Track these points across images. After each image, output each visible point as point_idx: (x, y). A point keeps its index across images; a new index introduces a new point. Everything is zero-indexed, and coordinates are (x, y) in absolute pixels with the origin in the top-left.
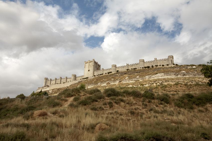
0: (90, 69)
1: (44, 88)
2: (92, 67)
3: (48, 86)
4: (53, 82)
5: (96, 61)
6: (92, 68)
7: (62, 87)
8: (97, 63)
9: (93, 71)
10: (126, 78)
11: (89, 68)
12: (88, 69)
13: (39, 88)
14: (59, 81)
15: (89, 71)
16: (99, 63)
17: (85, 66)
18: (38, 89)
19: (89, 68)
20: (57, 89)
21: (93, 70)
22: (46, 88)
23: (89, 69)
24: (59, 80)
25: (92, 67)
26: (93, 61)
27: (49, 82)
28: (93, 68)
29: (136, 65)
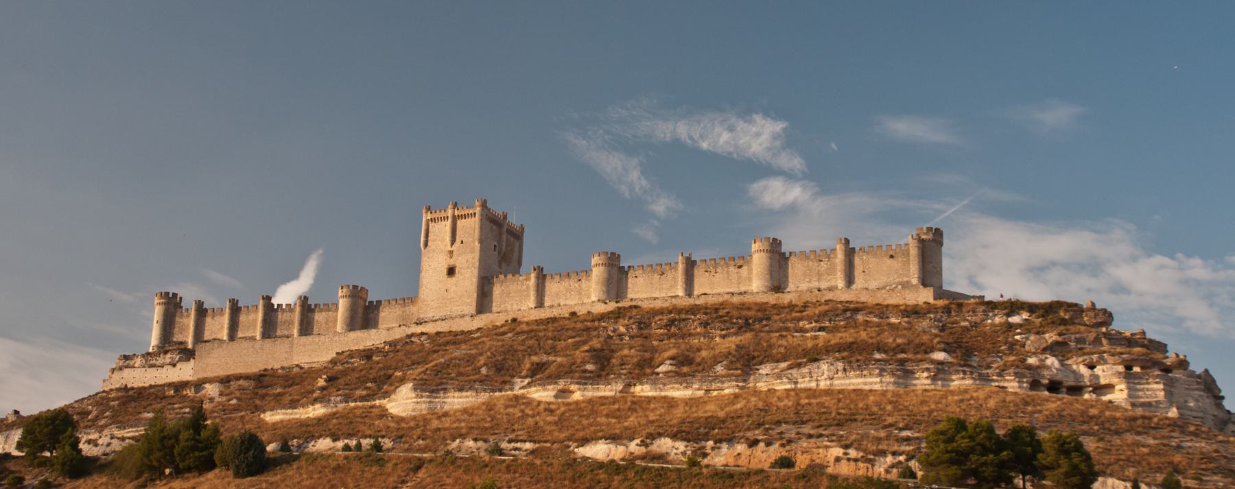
0: (460, 262)
1: (160, 361)
2: (472, 251)
3: (188, 354)
4: (218, 327)
5: (497, 209)
6: (470, 256)
7: (277, 366)
8: (505, 217)
9: (475, 280)
10: (659, 370)
11: (451, 252)
12: (443, 263)
13: (126, 358)
14: (255, 320)
15: (451, 271)
16: (514, 220)
17: (427, 236)
18: (121, 369)
19: (451, 252)
20: (247, 377)
21: (476, 272)
22: (174, 365)
23: (452, 262)
24: (252, 317)
25: (472, 251)
26: (478, 210)
27: (191, 322)
28: (477, 255)
29: (732, 269)
